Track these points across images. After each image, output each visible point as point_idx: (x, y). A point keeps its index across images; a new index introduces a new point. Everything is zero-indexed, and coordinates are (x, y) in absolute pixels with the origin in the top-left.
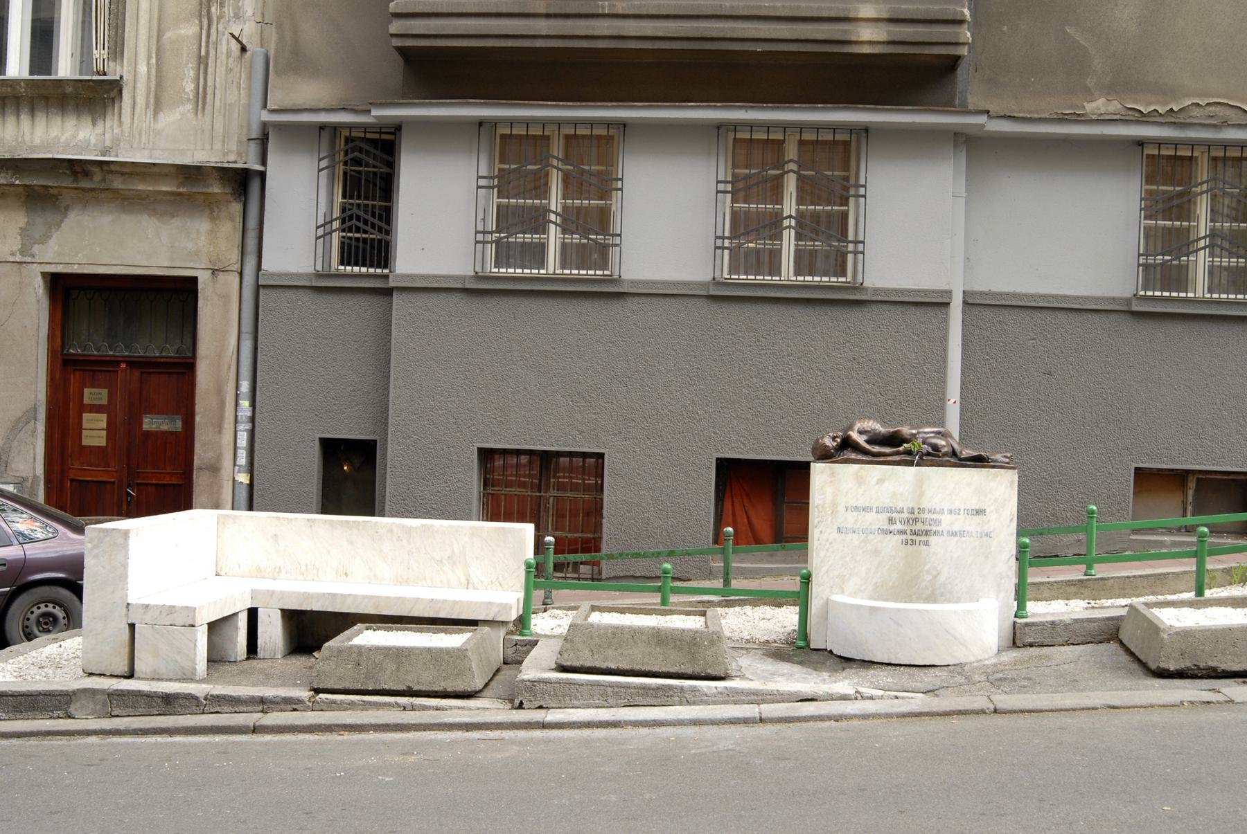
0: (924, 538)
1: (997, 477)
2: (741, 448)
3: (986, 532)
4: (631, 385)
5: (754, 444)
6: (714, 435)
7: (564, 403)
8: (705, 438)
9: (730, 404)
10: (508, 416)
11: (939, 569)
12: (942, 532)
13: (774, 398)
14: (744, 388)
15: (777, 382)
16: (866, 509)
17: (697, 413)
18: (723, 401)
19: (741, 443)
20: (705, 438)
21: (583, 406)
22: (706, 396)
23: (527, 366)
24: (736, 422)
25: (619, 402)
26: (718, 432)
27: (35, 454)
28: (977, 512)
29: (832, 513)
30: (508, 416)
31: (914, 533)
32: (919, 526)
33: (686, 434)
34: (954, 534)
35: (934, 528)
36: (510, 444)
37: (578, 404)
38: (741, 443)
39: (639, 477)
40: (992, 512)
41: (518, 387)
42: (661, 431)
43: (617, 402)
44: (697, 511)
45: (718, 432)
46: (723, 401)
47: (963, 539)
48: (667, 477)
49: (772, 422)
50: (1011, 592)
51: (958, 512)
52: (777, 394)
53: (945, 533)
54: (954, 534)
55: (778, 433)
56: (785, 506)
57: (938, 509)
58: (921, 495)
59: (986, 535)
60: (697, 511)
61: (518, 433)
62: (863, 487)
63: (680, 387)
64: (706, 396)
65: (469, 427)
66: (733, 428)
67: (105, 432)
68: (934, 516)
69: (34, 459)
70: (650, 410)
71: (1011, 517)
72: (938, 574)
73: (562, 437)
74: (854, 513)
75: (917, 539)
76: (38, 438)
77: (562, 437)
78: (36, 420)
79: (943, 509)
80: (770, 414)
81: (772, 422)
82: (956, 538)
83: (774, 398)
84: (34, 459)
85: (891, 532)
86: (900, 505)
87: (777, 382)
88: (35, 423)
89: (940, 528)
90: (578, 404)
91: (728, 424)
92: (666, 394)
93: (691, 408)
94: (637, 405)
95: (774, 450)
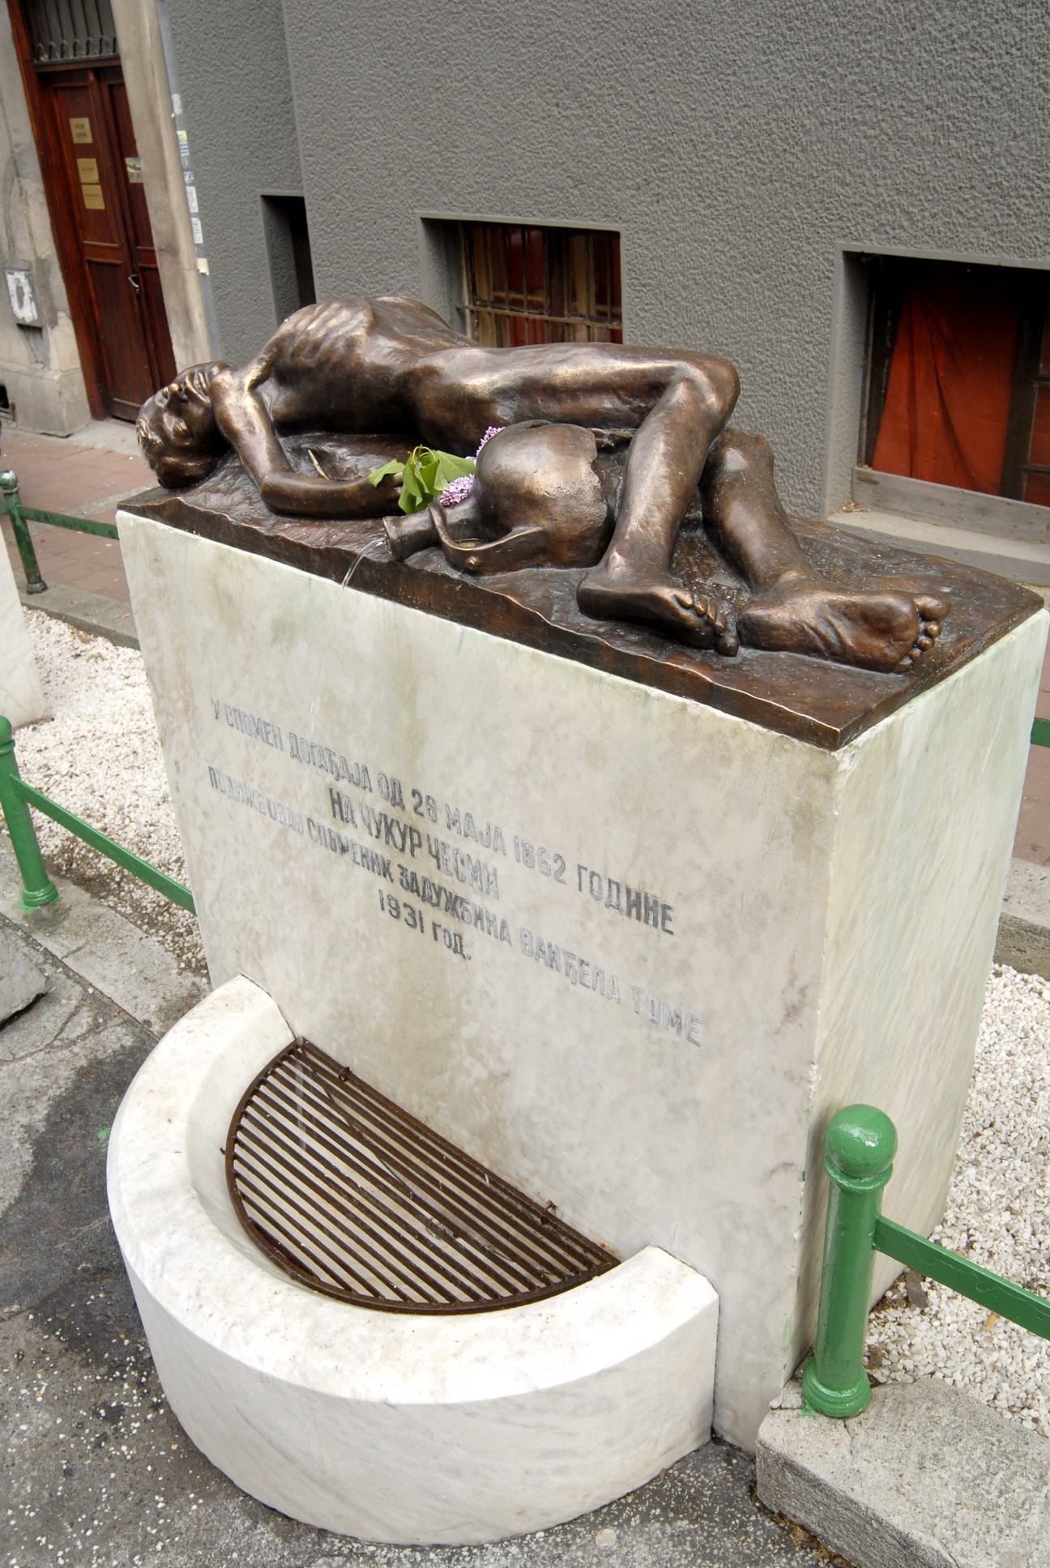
0: (446, 920)
1: (727, 760)
2: (902, 227)
3: (673, 1007)
4: (662, 56)
5: (934, 216)
6: (839, 189)
7: (544, 111)
8: (819, 197)
9: (880, 95)
10: (457, 147)
12: (504, 925)
13: (997, 71)
14: (918, 44)
15: (1011, 17)
16: (262, 730)
17: (804, 126)
18: (865, 88)
19: (904, 211)
20: (819, 197)
21: (578, 117)
22: (824, 75)
23: (475, 24)
24: (892, 149)
25: (642, 103)
26: (849, 179)
27: (29, 226)
29: (186, 711)
30: (457, 147)
31: (411, 884)
32: (422, 866)
33: (777, 185)
34: (548, 956)
35: (476, 900)
36: (466, 211)
37: (568, 113)
38: (904, 211)
39: (684, 294)
40: (699, 929)
41: (467, 78)
42: (725, 178)
43: (637, 102)
44: (799, 386)
45: (849, 179)
46: (865, 88)
47: (579, 988)
48: (738, 295)
49: (986, 150)
51: (556, 867)
52: (1006, 59)
53: (513, 931)
54: (548, 956)
55: (999, 184)
56: (1036, 385)
57: (480, 825)
58: (415, 739)
59: (676, 1021)
60: (799, 386)
61: (476, 186)
63: (765, 53)
64: (824, 75)
65: (405, 173)
66: (884, 168)
67: (99, 187)
68: (471, 848)
69: (31, 235)
70: (702, 122)
71: (793, 997)
72: (507, 1075)
73: (545, 193)
74: (234, 729)
75: (430, 914)
76: (31, 203)
77: (545, 193)
78: (18, 176)
79: (499, 834)
80: (982, 126)
81: (986, 150)
82: (555, 978)
83: (997, 71)
84: (31, 235)
85: (344, 850)
86: (356, 755)
87: (1011, 17)
88: (19, 182)
90: (568, 113)
91: (873, 157)
92: (734, 74)
93: (789, 114)
94: (675, 107)
95: (984, 234)
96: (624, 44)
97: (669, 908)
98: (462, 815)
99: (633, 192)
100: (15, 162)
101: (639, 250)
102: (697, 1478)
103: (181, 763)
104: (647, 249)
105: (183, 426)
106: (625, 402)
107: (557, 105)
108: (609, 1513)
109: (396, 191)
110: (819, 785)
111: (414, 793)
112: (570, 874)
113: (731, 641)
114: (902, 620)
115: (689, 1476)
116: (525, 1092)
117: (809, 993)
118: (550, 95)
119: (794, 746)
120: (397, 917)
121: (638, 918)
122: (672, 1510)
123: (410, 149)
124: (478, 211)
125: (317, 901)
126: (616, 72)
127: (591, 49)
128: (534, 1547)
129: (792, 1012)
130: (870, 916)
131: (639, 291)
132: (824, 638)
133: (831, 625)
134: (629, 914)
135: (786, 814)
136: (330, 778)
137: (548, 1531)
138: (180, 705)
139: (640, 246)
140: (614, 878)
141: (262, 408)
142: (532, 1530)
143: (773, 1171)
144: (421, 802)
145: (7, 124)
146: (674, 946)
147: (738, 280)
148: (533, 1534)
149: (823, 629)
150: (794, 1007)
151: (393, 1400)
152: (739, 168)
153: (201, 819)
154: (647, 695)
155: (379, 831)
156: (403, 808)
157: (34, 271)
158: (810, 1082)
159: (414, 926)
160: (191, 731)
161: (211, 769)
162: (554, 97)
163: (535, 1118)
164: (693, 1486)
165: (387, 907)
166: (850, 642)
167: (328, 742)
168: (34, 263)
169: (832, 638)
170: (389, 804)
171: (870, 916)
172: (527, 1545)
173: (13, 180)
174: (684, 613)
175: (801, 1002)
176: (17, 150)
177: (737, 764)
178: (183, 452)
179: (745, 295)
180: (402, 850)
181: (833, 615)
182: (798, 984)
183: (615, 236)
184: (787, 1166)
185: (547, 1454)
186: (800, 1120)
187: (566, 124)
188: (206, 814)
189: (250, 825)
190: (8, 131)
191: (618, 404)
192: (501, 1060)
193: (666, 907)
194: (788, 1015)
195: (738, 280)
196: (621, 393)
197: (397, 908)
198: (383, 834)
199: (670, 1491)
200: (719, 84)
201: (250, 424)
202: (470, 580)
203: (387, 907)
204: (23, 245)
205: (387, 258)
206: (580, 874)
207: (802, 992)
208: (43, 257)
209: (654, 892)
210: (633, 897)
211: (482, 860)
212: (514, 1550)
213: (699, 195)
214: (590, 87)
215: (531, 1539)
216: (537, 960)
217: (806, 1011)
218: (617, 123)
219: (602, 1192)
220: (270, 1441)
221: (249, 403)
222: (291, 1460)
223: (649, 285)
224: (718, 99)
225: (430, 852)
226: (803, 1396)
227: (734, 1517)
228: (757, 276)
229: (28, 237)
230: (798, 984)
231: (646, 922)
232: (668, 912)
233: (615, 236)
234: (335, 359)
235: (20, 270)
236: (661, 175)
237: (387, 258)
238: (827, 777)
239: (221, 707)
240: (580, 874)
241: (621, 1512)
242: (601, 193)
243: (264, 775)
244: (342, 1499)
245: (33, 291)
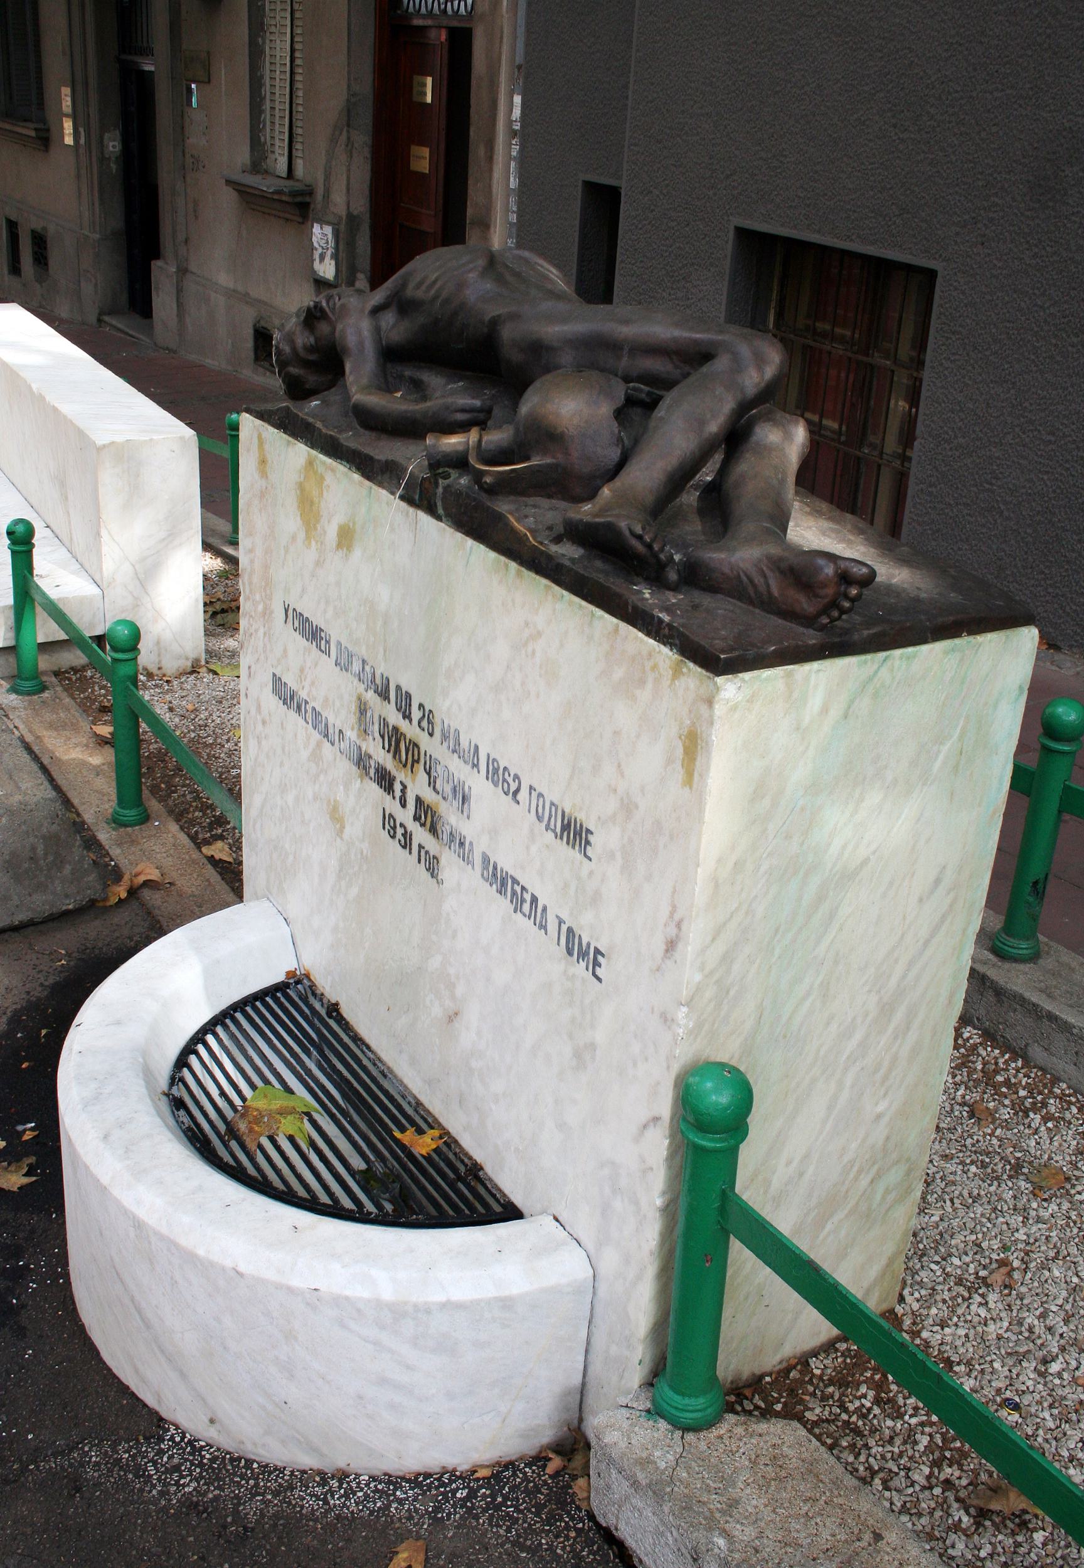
1: (642, 682)
10: (786, 156)
11: (460, 990)
25: (983, 134)
28: (566, 827)
29: (264, 614)
30: (786, 156)
40: (611, 856)
50: (639, 1277)
51: (513, 787)
62: (313, 543)
71: (672, 931)
75: (420, 835)
76: (355, 155)
88: (348, 132)
89: (467, 829)
96: (975, 70)
97: (592, 833)
98: (452, 731)
99: (958, 229)
100: (349, 111)
101: (954, 294)
102: (539, 1476)
103: (252, 670)
104: (963, 293)
105: (312, 340)
106: (676, 367)
107: (895, 126)
108: (439, 1479)
109: (715, 194)
110: (703, 709)
111: (421, 706)
112: (523, 795)
113: (673, 576)
114: (822, 577)
115: (533, 1472)
116: (468, 1035)
117: (684, 927)
118: (889, 114)
119: (689, 670)
120: (393, 837)
121: (568, 843)
122: (502, 1495)
123: (737, 152)
124: (795, 227)
125: (336, 816)
126: (962, 98)
127: (939, 70)
128: (354, 1485)
129: (671, 946)
130: (762, 870)
131: (947, 338)
132: (754, 586)
133: (765, 577)
134: (561, 838)
135: (680, 738)
136: (361, 687)
137: (373, 1478)
138: (260, 608)
139: (956, 289)
140: (556, 802)
141: (377, 330)
142: (359, 1472)
143: (645, 1126)
144: (424, 716)
145: (349, 73)
146: (591, 873)
147: (1054, 341)
148: (358, 1475)
149: (758, 580)
150: (672, 942)
151: (242, 1268)
152: (1073, 218)
153: (260, 727)
154: (593, 615)
155: (390, 745)
156: (411, 721)
157: (342, 227)
158: (679, 1026)
159: (404, 847)
160: (265, 634)
161: (274, 675)
162: (893, 117)
163: (474, 1064)
164: (533, 1481)
165: (387, 826)
166: (775, 592)
167: (363, 652)
168: (344, 218)
169: (762, 588)
170: (400, 716)
171: (762, 870)
172: (348, 1483)
173: (342, 130)
174: (634, 542)
175: (677, 936)
176: (353, 100)
177: (649, 686)
178: (306, 364)
179: (1058, 358)
180: (405, 766)
181: (768, 567)
182: (677, 917)
183: (932, 274)
184: (656, 1119)
185: (383, 1381)
186: (668, 1067)
187: (901, 147)
188: (264, 723)
189: (296, 735)
190: (349, 79)
191: (669, 367)
192: (453, 997)
193: (588, 831)
194: (667, 951)
195: (1054, 341)
196: (674, 357)
197: (394, 828)
198: (392, 748)
199: (508, 1479)
200: (1067, 125)
201: (361, 343)
202: (484, 497)
203: (387, 826)
204: (339, 199)
205: (693, 264)
206: (530, 794)
207: (679, 925)
208: (355, 213)
209: (581, 816)
210: (566, 822)
211: (462, 778)
212: (335, 1483)
213: (1028, 242)
214: (932, 111)
215: (355, 1479)
216: (491, 885)
217: (680, 946)
218: (954, 152)
219: (517, 1150)
220: (132, 1299)
221: (366, 325)
222: (148, 1326)
223: (959, 333)
224: (1063, 141)
225: (425, 769)
226: (654, 1401)
227: (561, 1519)
228: (1075, 340)
229: (344, 191)
230: (677, 917)
231: (573, 847)
232: (590, 837)
233: (932, 274)
234: (444, 294)
235: (328, 223)
236: (991, 215)
237: (693, 264)
238: (710, 702)
239: (290, 612)
240: (530, 794)
241: (451, 1481)
242: (924, 225)
243: (313, 683)
244: (183, 1375)
245: (337, 248)
